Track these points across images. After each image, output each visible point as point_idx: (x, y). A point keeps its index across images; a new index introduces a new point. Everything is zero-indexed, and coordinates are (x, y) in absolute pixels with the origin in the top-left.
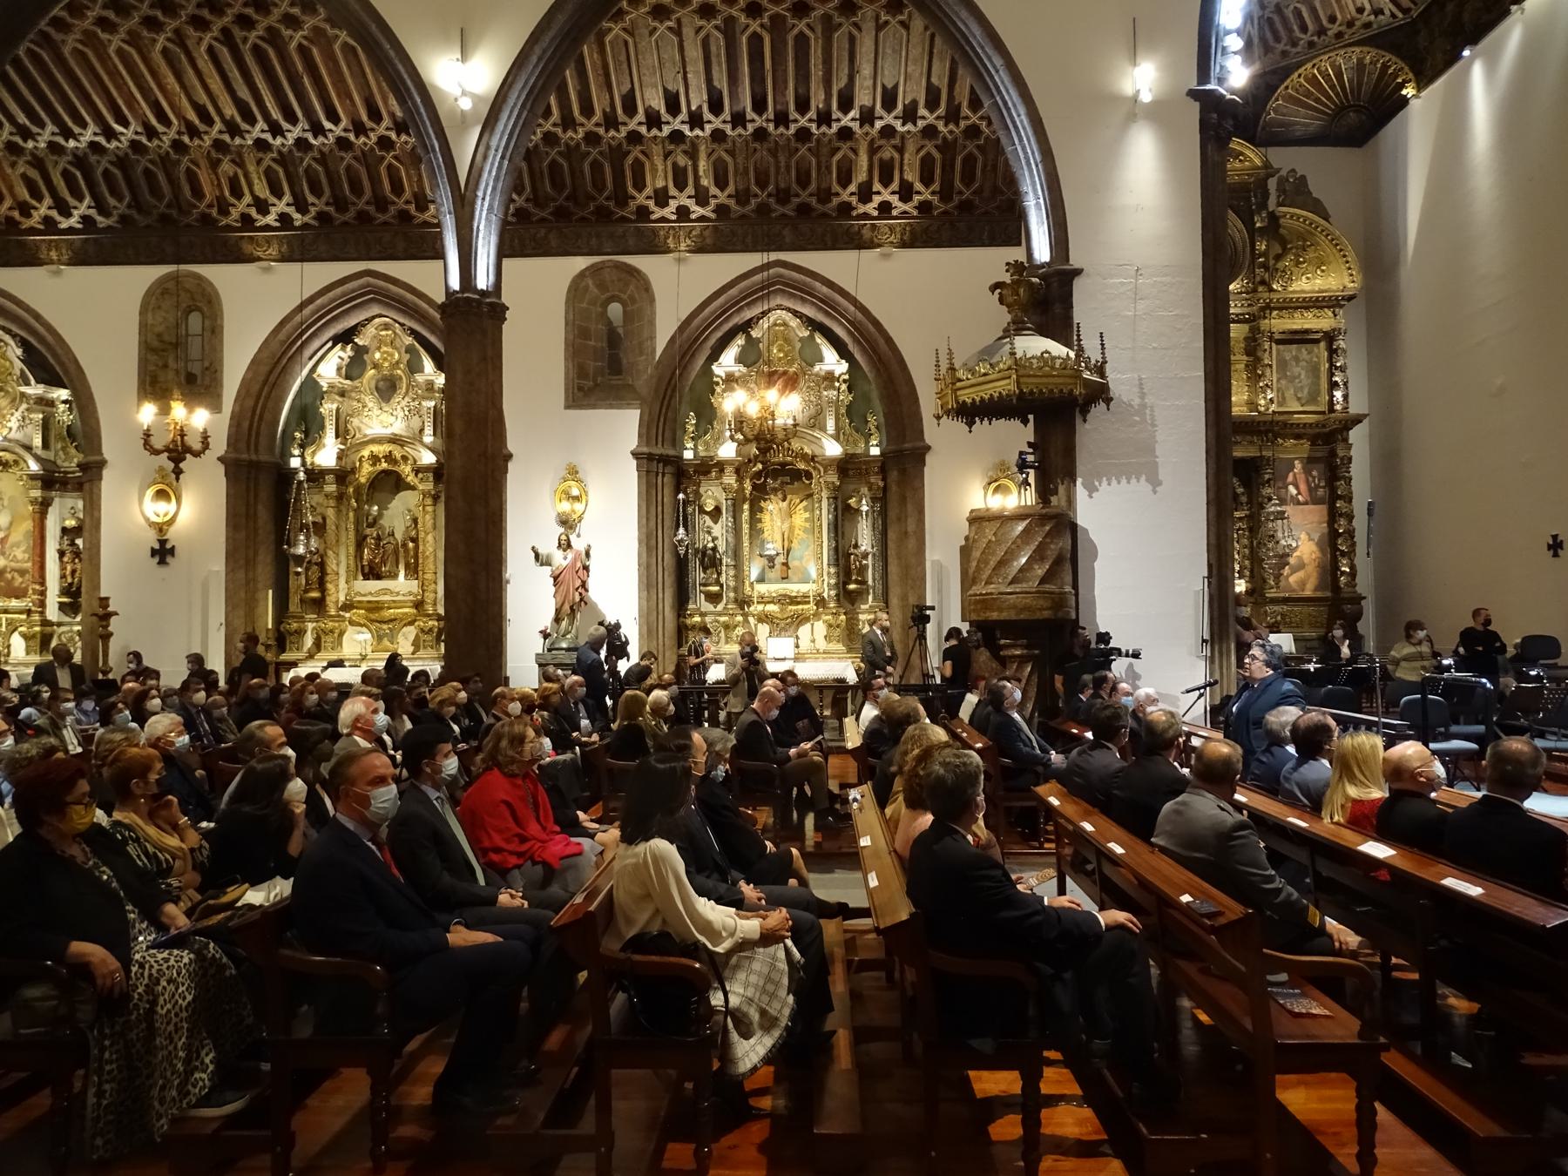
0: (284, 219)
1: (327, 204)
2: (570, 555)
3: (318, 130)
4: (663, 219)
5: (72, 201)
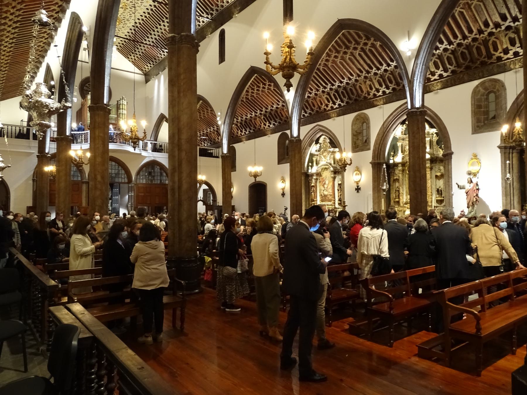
0: (384, 92)
2: (472, 185)
3: (389, 65)
4: (508, 59)
5: (336, 101)
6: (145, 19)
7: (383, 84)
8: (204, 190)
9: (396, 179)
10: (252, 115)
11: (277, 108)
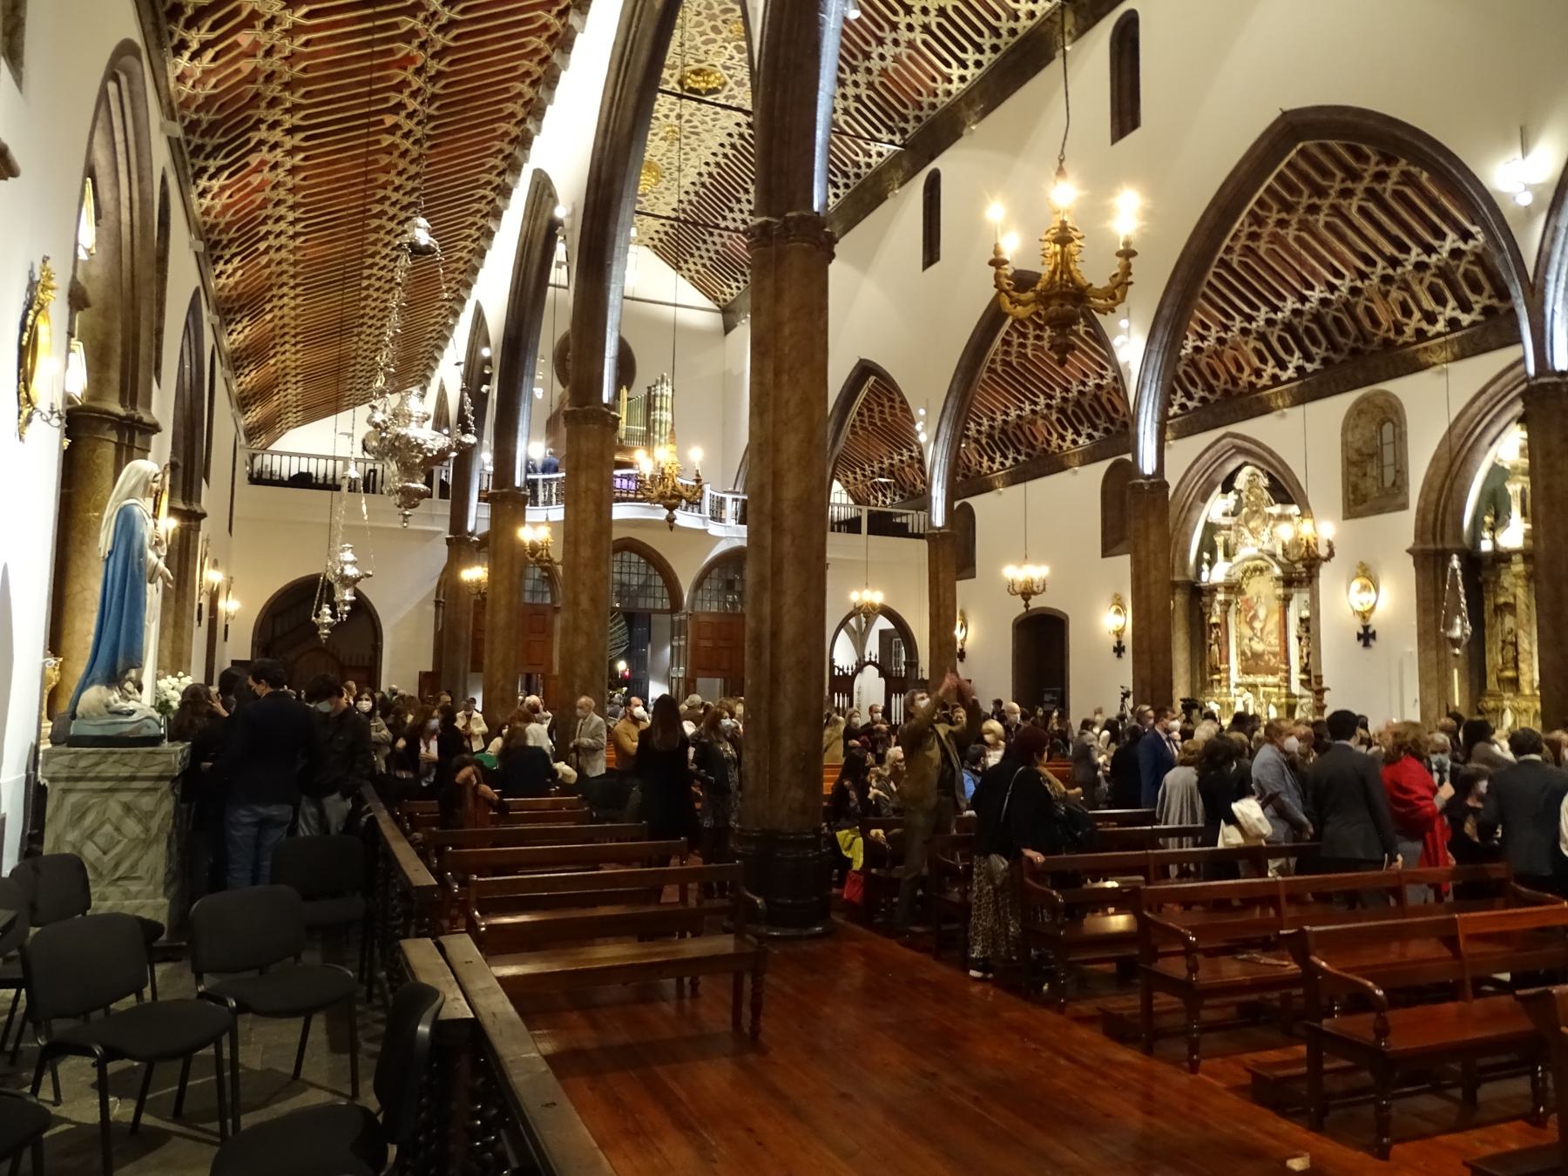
0: (1453, 324)
1: (1490, 297)
5: (1286, 357)
6: (722, 161)
7: (1448, 294)
8: (882, 633)
9: (1506, 604)
10: (1021, 409)
11: (1098, 386)
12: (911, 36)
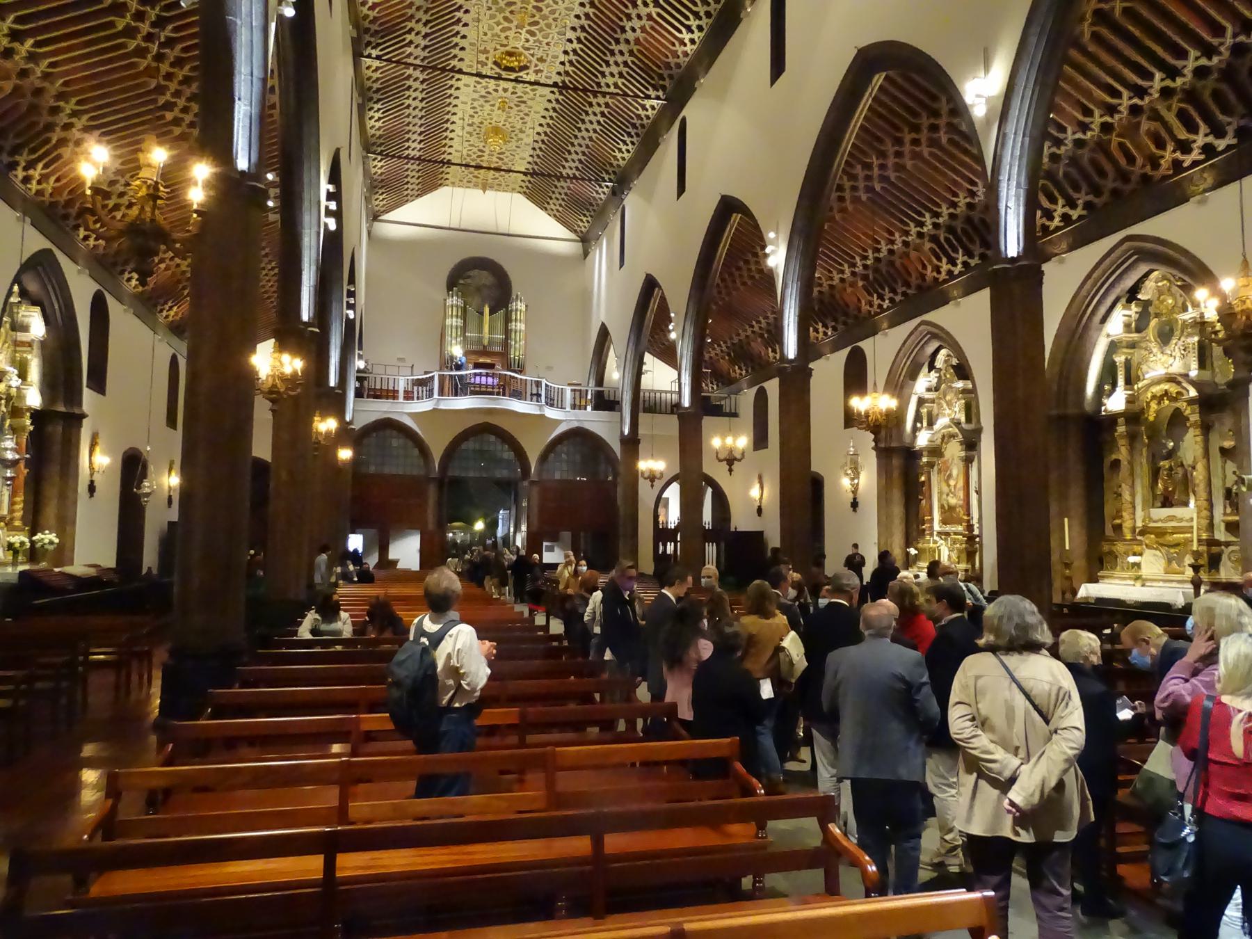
0: (1066, 218)
12: (648, 10)
